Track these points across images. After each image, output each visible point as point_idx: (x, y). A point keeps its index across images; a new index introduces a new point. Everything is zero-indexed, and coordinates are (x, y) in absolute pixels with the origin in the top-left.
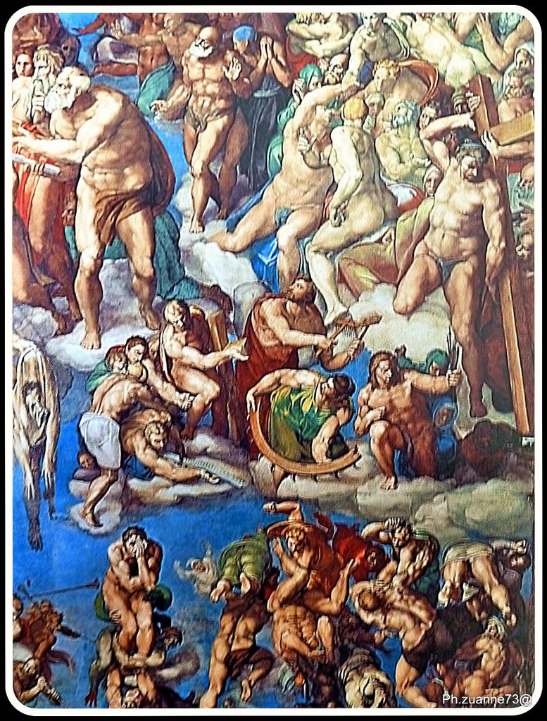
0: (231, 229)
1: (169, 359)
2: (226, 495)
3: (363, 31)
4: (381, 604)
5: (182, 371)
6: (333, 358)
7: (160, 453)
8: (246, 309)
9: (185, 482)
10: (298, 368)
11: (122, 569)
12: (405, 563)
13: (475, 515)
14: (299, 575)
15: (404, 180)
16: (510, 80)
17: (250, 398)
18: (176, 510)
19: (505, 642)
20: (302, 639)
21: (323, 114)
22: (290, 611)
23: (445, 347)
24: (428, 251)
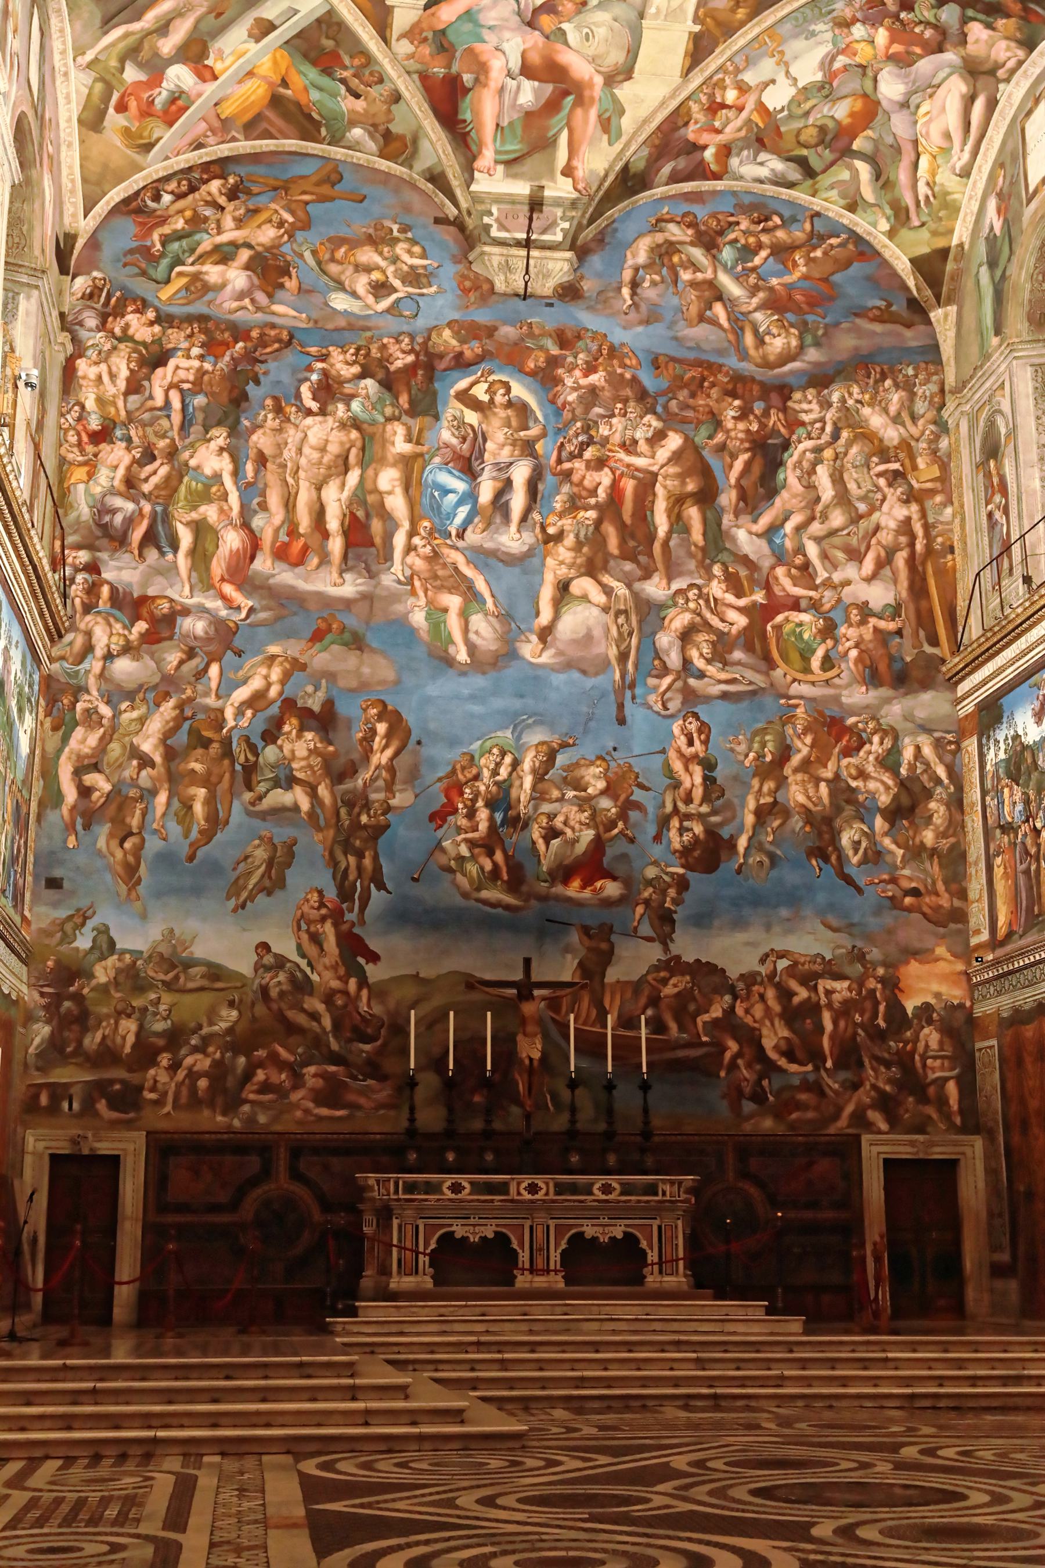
0: (755, 521)
1: (715, 599)
2: (754, 693)
3: (833, 410)
4: (862, 774)
5: (724, 608)
7: (709, 661)
8: (765, 571)
9: (727, 682)
11: (682, 741)
12: (876, 746)
13: (921, 714)
14: (805, 751)
15: (863, 499)
16: (924, 445)
17: (769, 628)
19: (948, 805)
20: (809, 798)
22: (799, 777)
23: (893, 603)
24: (879, 543)
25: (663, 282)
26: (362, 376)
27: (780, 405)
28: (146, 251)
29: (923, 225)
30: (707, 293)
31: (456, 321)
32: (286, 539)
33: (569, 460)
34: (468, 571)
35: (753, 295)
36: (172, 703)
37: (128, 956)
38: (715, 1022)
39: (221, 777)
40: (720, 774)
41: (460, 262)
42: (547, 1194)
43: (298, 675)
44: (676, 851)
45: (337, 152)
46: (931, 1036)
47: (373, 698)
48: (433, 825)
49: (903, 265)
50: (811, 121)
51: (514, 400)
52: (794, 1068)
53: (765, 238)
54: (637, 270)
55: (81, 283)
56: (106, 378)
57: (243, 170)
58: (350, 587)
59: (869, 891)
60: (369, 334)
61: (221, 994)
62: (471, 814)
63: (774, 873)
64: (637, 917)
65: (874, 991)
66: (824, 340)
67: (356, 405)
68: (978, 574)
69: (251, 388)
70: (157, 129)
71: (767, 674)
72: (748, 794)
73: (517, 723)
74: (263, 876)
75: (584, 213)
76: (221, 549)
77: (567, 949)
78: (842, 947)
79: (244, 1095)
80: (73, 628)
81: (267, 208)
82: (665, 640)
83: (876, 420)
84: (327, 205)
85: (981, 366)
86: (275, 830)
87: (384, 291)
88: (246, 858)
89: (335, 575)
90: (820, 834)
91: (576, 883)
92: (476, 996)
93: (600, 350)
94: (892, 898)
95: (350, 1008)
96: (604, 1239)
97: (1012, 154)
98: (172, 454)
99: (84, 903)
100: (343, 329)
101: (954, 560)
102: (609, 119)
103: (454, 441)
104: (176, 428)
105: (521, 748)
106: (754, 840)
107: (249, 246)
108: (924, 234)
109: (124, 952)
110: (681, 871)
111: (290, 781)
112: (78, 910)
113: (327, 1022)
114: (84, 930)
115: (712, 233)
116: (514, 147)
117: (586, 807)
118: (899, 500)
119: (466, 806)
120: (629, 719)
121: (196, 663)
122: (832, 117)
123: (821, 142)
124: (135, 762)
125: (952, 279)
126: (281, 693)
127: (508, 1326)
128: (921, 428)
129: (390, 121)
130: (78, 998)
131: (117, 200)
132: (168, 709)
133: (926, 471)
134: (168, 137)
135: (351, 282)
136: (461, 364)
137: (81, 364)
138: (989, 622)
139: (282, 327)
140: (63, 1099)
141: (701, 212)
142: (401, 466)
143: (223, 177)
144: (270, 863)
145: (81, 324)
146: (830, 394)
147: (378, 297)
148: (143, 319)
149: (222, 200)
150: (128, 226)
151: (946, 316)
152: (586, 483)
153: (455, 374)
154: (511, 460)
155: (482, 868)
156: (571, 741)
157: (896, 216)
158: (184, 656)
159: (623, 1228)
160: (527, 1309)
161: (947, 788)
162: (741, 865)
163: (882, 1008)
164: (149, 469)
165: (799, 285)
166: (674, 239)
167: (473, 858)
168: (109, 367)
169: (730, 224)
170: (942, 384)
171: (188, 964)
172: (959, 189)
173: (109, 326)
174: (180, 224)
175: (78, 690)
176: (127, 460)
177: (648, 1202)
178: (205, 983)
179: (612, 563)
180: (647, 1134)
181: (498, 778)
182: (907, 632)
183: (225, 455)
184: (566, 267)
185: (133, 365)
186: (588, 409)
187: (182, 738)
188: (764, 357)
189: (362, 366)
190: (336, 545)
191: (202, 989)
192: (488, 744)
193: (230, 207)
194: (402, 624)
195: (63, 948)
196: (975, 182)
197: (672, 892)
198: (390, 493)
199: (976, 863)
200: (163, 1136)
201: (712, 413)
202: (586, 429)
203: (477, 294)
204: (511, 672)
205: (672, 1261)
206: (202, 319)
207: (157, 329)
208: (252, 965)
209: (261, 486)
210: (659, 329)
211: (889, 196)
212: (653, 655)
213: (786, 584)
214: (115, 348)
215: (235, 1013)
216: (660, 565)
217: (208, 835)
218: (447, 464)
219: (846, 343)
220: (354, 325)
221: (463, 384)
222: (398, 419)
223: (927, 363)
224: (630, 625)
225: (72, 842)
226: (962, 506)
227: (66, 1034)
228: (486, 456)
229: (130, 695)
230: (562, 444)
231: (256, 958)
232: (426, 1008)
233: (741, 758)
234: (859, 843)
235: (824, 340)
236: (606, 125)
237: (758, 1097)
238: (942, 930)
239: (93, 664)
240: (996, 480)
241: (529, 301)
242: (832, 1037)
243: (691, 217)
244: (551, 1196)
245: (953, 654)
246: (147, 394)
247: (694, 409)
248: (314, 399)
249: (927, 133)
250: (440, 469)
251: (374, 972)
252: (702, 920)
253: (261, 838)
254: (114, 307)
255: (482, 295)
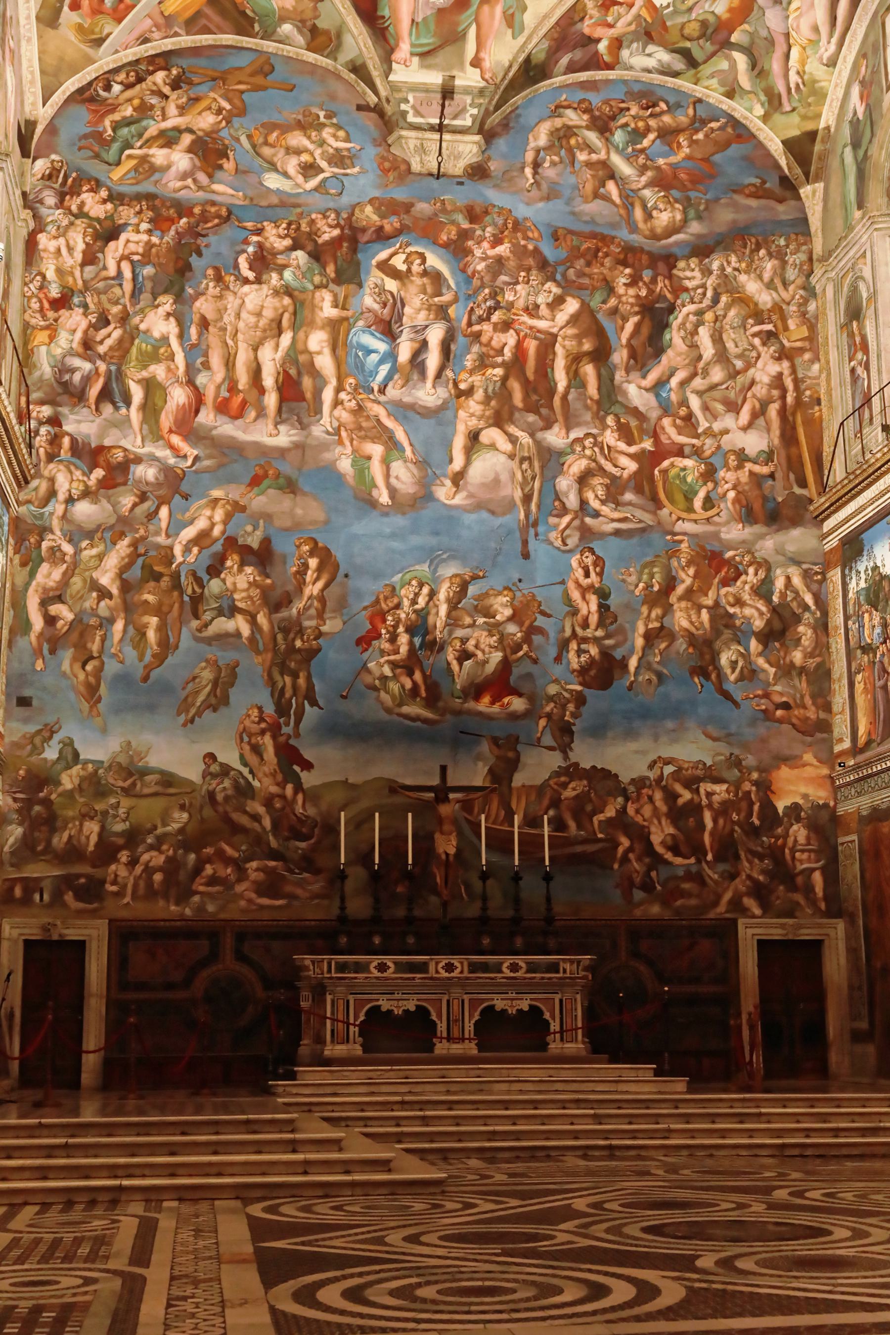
0: (644, 377)
1: (609, 447)
2: (643, 530)
4: (739, 602)
5: (617, 455)
6: (704, 452)
7: (603, 502)
8: (653, 422)
9: (620, 520)
10: (684, 457)
11: (579, 573)
12: (751, 577)
13: (791, 548)
14: (688, 581)
15: (740, 356)
16: (793, 308)
17: (656, 472)
18: (613, 538)
20: (692, 623)
21: (692, 318)
22: (683, 604)
23: (766, 449)
24: (754, 396)
25: (561, 162)
26: (294, 248)
27: (666, 273)
28: (98, 136)
29: (794, 110)
30: (600, 173)
31: (377, 198)
32: (227, 395)
33: (479, 323)
34: (389, 423)
35: (642, 174)
36: (126, 541)
37: (90, 766)
38: (609, 820)
39: (172, 607)
40: (614, 602)
41: (380, 145)
42: (462, 972)
43: (238, 515)
44: (574, 671)
45: (269, 46)
46: (799, 833)
47: (306, 536)
48: (360, 649)
49: (776, 147)
50: (694, 16)
51: (429, 269)
52: (679, 860)
53: (652, 123)
54: (538, 151)
55: (41, 166)
56: (64, 251)
57: (185, 63)
58: (285, 437)
59: (744, 705)
60: (299, 210)
61: (173, 798)
62: (393, 639)
63: (662, 689)
64: (540, 728)
65: (749, 793)
66: (705, 214)
67: (288, 274)
68: (842, 424)
69: (194, 260)
70: (107, 26)
71: (655, 513)
72: (638, 619)
73: (434, 558)
74: (209, 695)
75: (491, 100)
76: (169, 403)
77: (479, 757)
78: (722, 755)
79: (194, 887)
80: (38, 475)
81: (207, 97)
82: (564, 483)
83: (751, 286)
84: (261, 93)
85: (846, 237)
86: (219, 654)
87: (312, 172)
88: (194, 678)
89: (271, 427)
90: (702, 655)
91: (486, 699)
92: (398, 799)
93: (505, 224)
94: (764, 711)
95: (288, 810)
96: (512, 1011)
97: (873, 45)
98: (124, 318)
99: (51, 719)
100: (276, 206)
101: (820, 410)
102: (513, 15)
103: (376, 307)
104: (127, 295)
105: (437, 580)
106: (644, 660)
107: (190, 131)
108: (795, 118)
109: (87, 762)
110: (579, 688)
111: (232, 611)
112: (46, 725)
113: (267, 822)
114: (51, 743)
115: (606, 119)
116: (428, 41)
117: (495, 632)
118: (772, 357)
119: (388, 632)
120: (532, 553)
121: (146, 505)
122: (713, 12)
123: (703, 35)
124: (94, 594)
125: (820, 158)
126: (224, 532)
127: (428, 1088)
128: (791, 292)
129: (316, 17)
130: (47, 803)
131: (73, 89)
132: (123, 547)
133: (796, 331)
134: (117, 32)
135: (283, 163)
136: (382, 237)
137: (42, 238)
138: (852, 467)
139: (221, 205)
140: (34, 892)
141: (595, 99)
142: (328, 329)
143: (167, 69)
144: (215, 683)
145: (41, 202)
146: (711, 263)
147: (306, 177)
148: (97, 197)
149: (166, 90)
150: (82, 113)
151: (814, 192)
152: (494, 343)
153: (376, 246)
154: (427, 323)
155: (403, 687)
156: (481, 574)
157: (770, 102)
158: (137, 500)
159: (529, 1002)
160: (444, 1072)
161: (814, 613)
162: (632, 683)
163: (756, 807)
164: (103, 332)
165: (683, 164)
166: (571, 123)
167: (395, 677)
168: (67, 241)
169: (622, 110)
170: (810, 253)
171: (145, 772)
172: (826, 77)
173: (66, 203)
174: (128, 111)
175: (44, 531)
176: (84, 324)
177: (550, 978)
178: (158, 789)
179: (517, 415)
180: (550, 920)
181: (416, 607)
182: (779, 475)
183: (172, 319)
184: (475, 149)
185: (88, 239)
186: (495, 276)
187: (136, 572)
188: (652, 230)
189: (293, 239)
190: (271, 400)
191: (155, 794)
192: (408, 577)
193: (174, 96)
194: (331, 473)
195: (34, 759)
196: (840, 72)
197: (571, 707)
198: (319, 353)
199: (839, 680)
200: (123, 923)
201: (605, 280)
202: (494, 295)
203: (396, 173)
204: (428, 513)
205: (572, 1030)
206: (150, 197)
207: (109, 206)
208: (200, 773)
209: (204, 347)
210: (558, 205)
211: (763, 84)
212: (554, 497)
213: (671, 433)
214: (72, 224)
215: (185, 816)
216: (560, 417)
217: (160, 658)
218: (369, 327)
219: (725, 217)
220: (286, 202)
221: (383, 255)
222: (326, 287)
223: (797, 234)
224: (533, 471)
225: (39, 665)
226: (828, 362)
227: (37, 834)
228: (405, 319)
229: (90, 535)
230: (472, 309)
231: (204, 767)
232: (354, 810)
233: (632, 588)
234: (736, 662)
235: (705, 214)
236: (510, 20)
237: (647, 886)
238: (809, 739)
239: (57, 507)
240: (858, 339)
241: (441, 180)
242: (712, 834)
243: (587, 104)
244: (466, 974)
245: (819, 494)
246: (101, 265)
247: (590, 276)
248: (250, 269)
249: (798, 26)
250: (364, 332)
251: (309, 779)
252: (598, 731)
253: (207, 661)
254: (71, 187)
255: (400, 174)
